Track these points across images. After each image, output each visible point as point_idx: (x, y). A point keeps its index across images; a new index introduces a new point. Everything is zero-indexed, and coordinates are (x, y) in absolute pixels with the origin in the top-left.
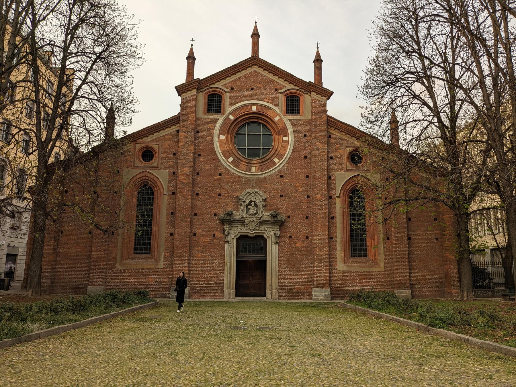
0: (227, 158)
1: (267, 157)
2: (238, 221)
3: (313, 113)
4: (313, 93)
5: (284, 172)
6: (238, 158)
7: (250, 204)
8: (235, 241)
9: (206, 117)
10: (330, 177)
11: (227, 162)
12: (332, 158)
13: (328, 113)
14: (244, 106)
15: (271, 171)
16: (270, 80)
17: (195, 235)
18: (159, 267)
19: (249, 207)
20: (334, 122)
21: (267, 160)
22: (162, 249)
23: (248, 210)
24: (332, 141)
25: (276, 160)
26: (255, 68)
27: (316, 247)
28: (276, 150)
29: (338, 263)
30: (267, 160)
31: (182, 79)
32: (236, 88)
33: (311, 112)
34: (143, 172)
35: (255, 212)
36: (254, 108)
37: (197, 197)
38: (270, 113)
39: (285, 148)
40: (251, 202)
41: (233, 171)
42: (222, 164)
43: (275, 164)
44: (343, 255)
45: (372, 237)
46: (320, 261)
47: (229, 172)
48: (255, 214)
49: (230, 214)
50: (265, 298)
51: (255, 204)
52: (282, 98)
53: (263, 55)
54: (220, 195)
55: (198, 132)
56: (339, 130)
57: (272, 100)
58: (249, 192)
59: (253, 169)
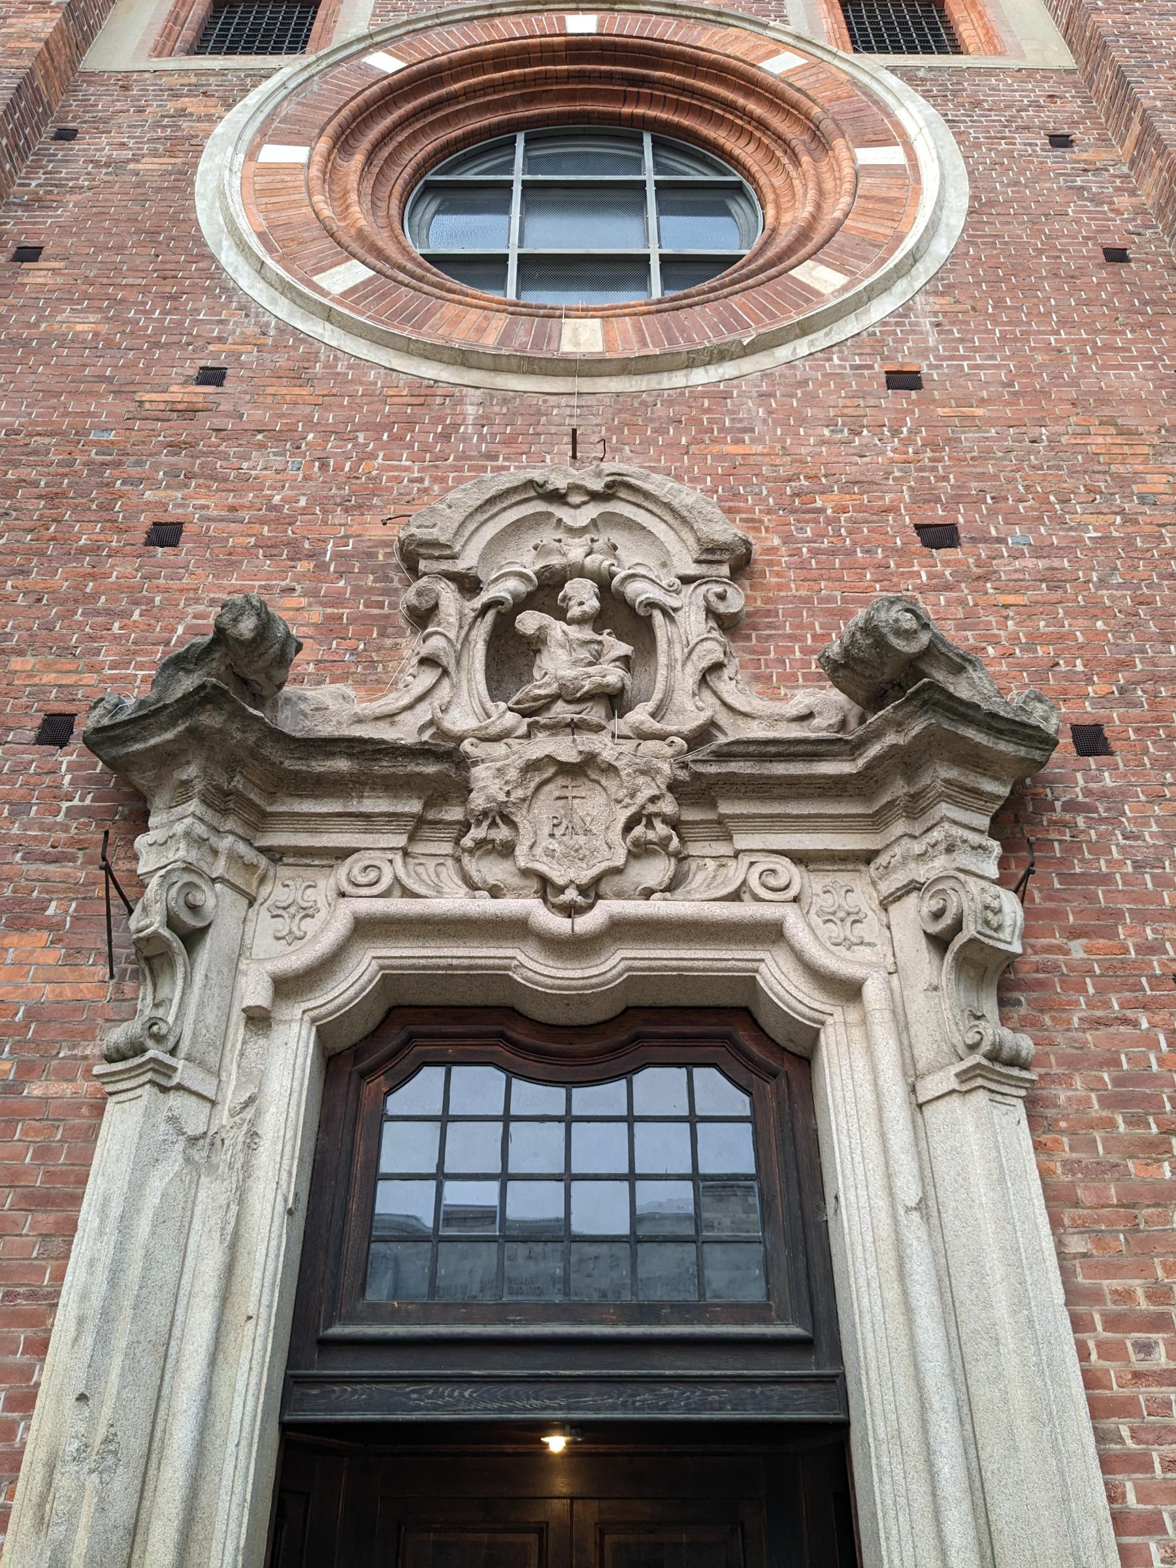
2: (369, 763)
5: (923, 352)
7: (547, 590)
19: (529, 622)
23: (510, 654)
42: (247, 307)
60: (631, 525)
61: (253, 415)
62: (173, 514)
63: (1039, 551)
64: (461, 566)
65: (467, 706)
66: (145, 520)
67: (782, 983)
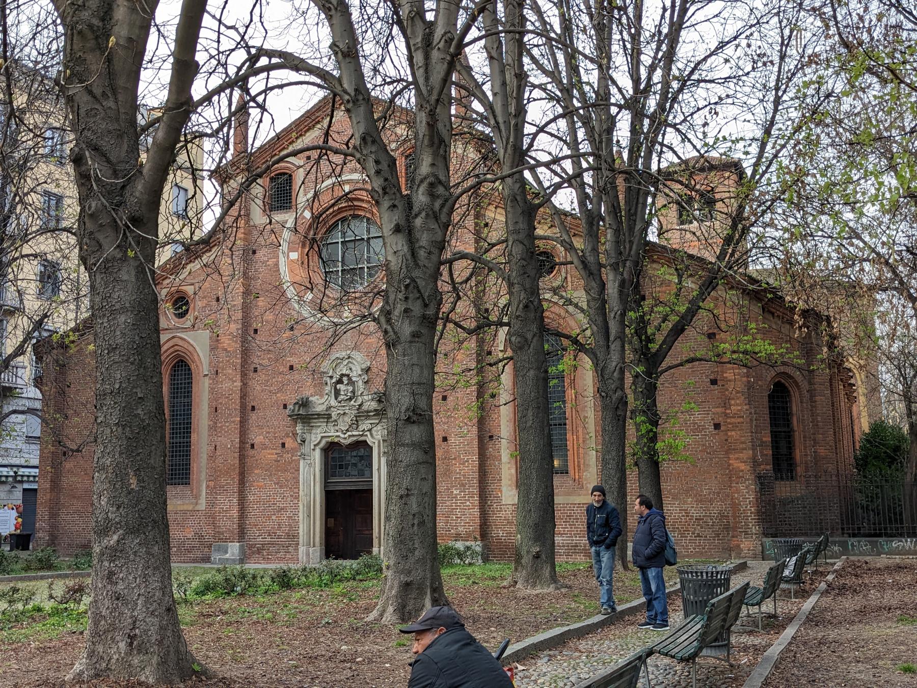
7: (340, 381)
8: (317, 455)
17: (253, 446)
18: (198, 507)
19: (338, 386)
22: (203, 476)
27: (455, 459)
29: (504, 489)
34: (173, 337)
37: (255, 375)
44: (513, 471)
45: (575, 432)
46: (463, 485)
48: (350, 399)
49: (305, 403)
51: (350, 379)
54: (291, 368)
55: (254, 252)
65: (333, 402)
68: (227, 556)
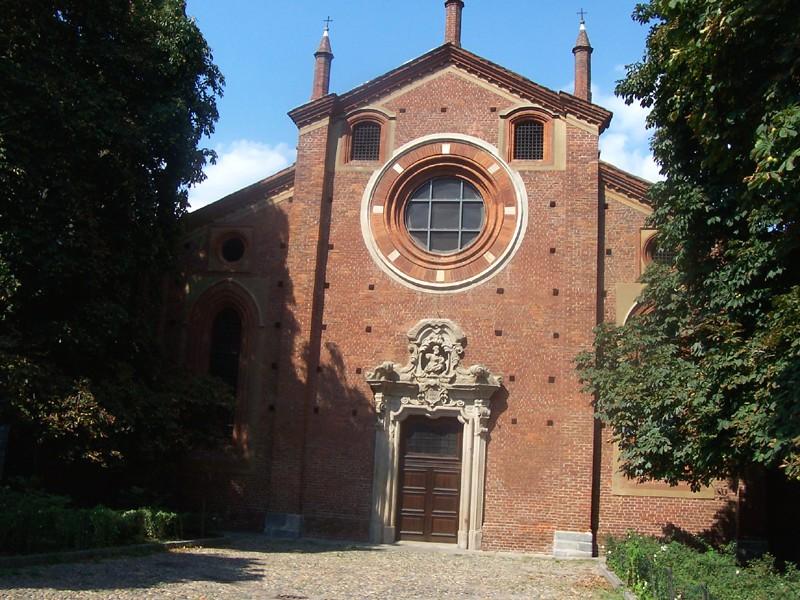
0: (387, 252)
1: (468, 253)
3: (571, 157)
4: (568, 115)
6: (409, 251)
7: (430, 350)
9: (348, 169)
10: (601, 294)
11: (385, 263)
12: (609, 252)
13: (603, 158)
14: (424, 144)
15: (477, 282)
16: (482, 91)
19: (428, 356)
20: (614, 176)
21: (472, 255)
24: (608, 215)
25: (489, 257)
26: (452, 69)
28: (491, 236)
30: (472, 255)
31: (306, 96)
32: (411, 110)
33: (568, 155)
35: (440, 366)
36: (446, 149)
38: (478, 159)
39: (510, 230)
40: (432, 344)
41: (396, 278)
42: (375, 265)
43: (486, 264)
46: (574, 473)
47: (389, 282)
48: (441, 371)
50: (455, 545)
52: (504, 128)
53: (470, 44)
54: (369, 330)
56: (625, 193)
57: (485, 132)
58: (429, 326)
59: (440, 275)
60: (445, 332)
61: (381, 299)
62: (369, 325)
63: (516, 337)
64: (418, 341)
65: (420, 372)
66: (366, 326)
67: (460, 418)
68: (284, 528)
